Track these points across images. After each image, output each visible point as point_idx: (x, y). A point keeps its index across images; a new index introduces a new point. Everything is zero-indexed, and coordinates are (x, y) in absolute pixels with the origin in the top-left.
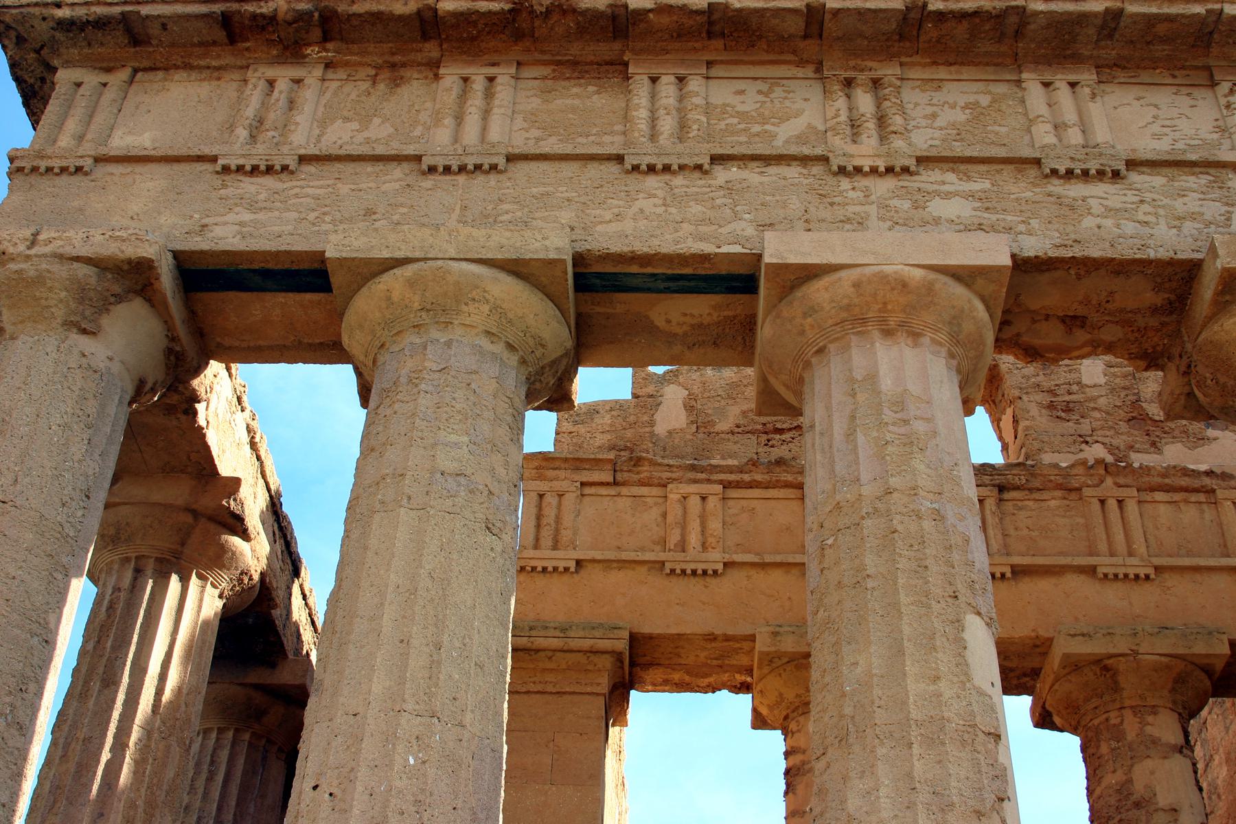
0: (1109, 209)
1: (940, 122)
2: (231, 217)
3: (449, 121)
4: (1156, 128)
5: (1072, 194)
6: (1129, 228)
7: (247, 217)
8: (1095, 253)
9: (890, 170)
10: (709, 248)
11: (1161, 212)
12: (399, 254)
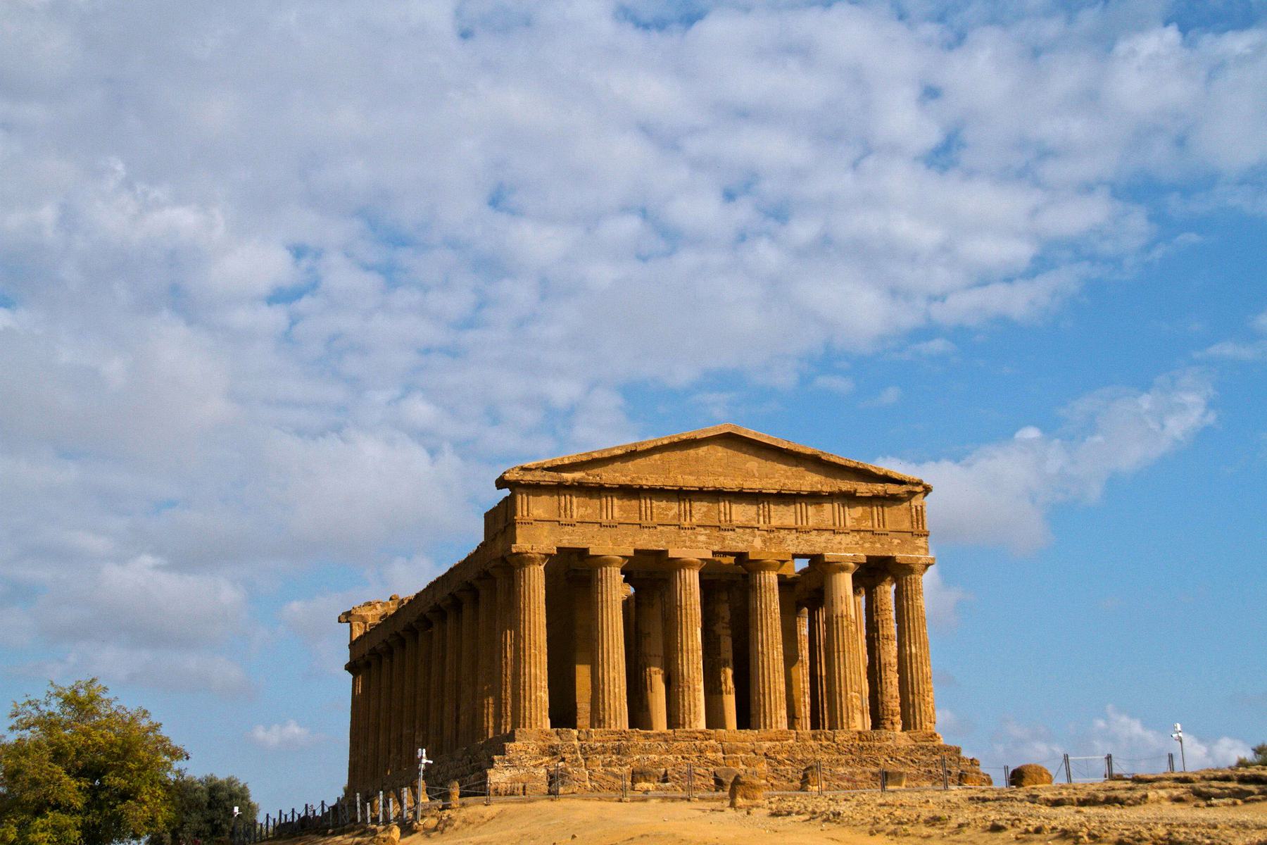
1: (701, 512)
2: (565, 537)
6: (734, 543)
10: (657, 549)
12: (601, 554)
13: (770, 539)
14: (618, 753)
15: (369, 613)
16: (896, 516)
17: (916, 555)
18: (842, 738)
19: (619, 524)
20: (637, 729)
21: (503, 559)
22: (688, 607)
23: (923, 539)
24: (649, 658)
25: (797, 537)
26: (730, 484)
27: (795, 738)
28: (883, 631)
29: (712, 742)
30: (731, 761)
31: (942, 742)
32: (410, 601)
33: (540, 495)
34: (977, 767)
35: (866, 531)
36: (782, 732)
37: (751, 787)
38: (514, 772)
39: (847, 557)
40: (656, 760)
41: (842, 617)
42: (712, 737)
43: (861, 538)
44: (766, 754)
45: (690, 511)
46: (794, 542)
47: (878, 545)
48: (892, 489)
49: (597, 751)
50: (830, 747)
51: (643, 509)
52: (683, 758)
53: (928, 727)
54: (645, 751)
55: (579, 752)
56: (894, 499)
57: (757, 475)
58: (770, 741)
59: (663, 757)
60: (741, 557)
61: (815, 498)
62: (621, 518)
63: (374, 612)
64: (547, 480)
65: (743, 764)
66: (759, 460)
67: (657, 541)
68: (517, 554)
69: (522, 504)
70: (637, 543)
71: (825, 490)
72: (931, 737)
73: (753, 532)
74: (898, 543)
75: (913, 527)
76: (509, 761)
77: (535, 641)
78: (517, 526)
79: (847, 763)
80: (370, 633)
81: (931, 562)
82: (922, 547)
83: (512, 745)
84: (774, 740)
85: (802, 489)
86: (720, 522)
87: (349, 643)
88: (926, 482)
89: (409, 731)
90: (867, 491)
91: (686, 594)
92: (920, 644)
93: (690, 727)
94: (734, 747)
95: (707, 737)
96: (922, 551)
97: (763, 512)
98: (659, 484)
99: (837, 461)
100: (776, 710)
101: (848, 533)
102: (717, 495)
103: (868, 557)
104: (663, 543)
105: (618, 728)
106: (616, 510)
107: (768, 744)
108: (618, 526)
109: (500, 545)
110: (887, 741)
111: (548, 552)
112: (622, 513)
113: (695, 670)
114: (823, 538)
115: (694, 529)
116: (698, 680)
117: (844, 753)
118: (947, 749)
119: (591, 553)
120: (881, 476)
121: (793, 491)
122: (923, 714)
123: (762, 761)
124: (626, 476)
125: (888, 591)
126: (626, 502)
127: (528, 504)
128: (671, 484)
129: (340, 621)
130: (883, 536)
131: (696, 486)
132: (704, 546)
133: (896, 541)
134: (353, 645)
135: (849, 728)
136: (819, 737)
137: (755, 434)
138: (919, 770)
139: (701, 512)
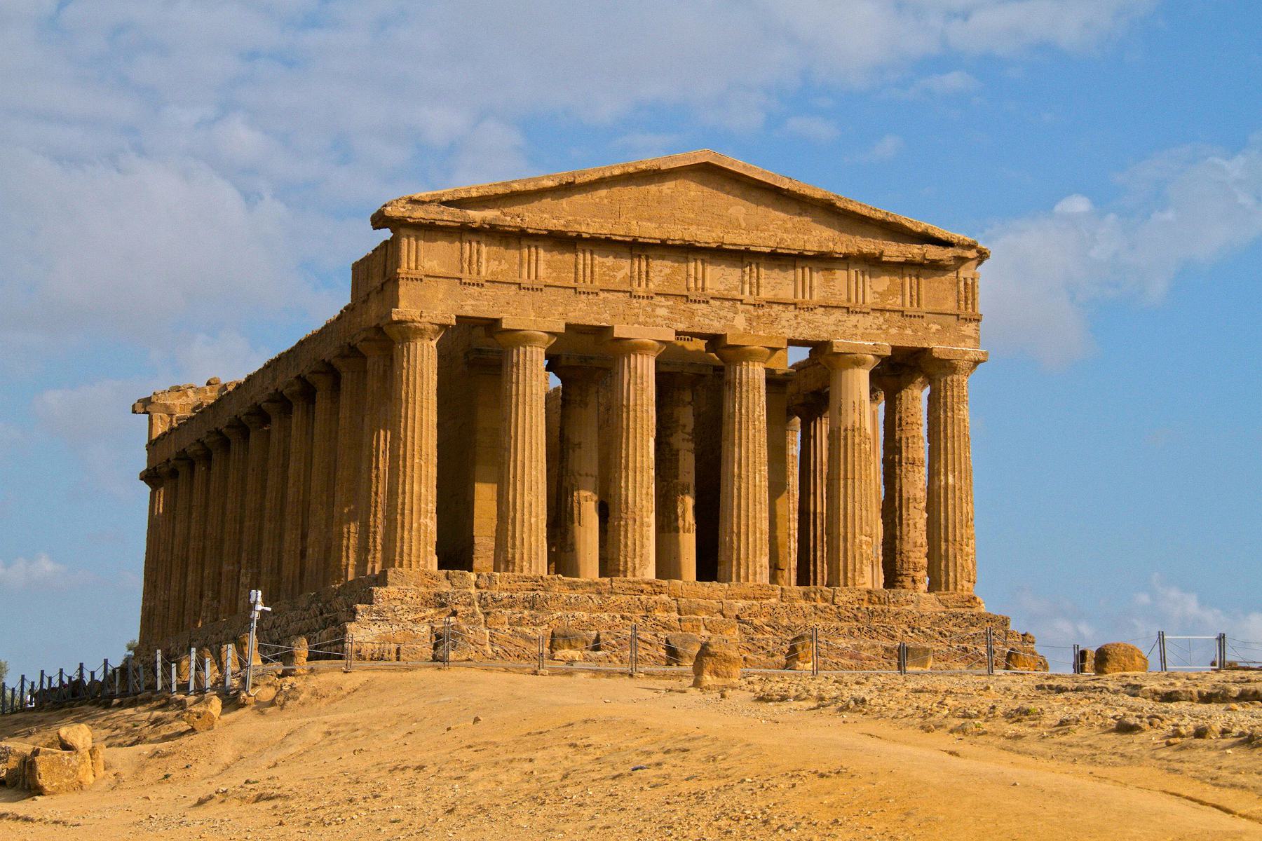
1: (662, 275)
2: (468, 302)
3: (526, 265)
4: (722, 280)
6: (707, 321)
7: (473, 303)
9: (648, 297)
10: (598, 324)
13: (758, 317)
14: (532, 608)
15: (177, 402)
16: (938, 292)
17: (962, 347)
18: (845, 599)
19: (545, 286)
20: (560, 576)
21: (379, 329)
22: (638, 407)
23: (972, 325)
24: (578, 477)
26: (706, 236)
27: (779, 596)
28: (907, 452)
29: (664, 597)
30: (689, 625)
31: (983, 609)
32: (239, 386)
33: (436, 240)
34: (1030, 646)
35: (894, 311)
36: (761, 587)
37: (725, 661)
38: (385, 628)
39: (865, 347)
40: (585, 619)
41: (853, 430)
42: (664, 590)
43: (886, 321)
44: (737, 617)
45: (647, 272)
46: (791, 322)
47: (909, 332)
48: (933, 252)
49: (501, 603)
50: (828, 610)
51: (581, 267)
52: (623, 617)
53: (965, 588)
54: (568, 605)
55: (477, 604)
56: (936, 267)
57: (743, 225)
58: (745, 599)
59: (594, 615)
60: (714, 341)
61: (824, 260)
62: (549, 278)
63: (183, 400)
64: (445, 218)
65: (706, 629)
66: (748, 204)
67: (598, 314)
68: (400, 322)
69: (409, 252)
70: (570, 314)
71: (838, 251)
72: (969, 601)
74: (937, 330)
75: (959, 308)
76: (378, 613)
77: (421, 447)
78: (401, 282)
79: (851, 633)
80: (177, 429)
81: (982, 358)
82: (970, 337)
83: (383, 590)
84: (750, 598)
85: (807, 248)
86: (688, 290)
87: (146, 442)
88: (981, 245)
89: (231, 568)
90: (897, 254)
91: (636, 390)
92: (960, 472)
93: (634, 576)
94: (694, 606)
95: (657, 590)
96: (970, 342)
97: (750, 277)
98: (606, 232)
99: (858, 209)
100: (755, 557)
101: (868, 313)
102: (687, 251)
103: (894, 349)
104: (607, 316)
105: (533, 573)
106: (542, 266)
107: (741, 603)
108: (544, 289)
109: (374, 309)
110: (907, 605)
111: (444, 321)
112: (550, 270)
113: (644, 496)
114: (832, 319)
115: (652, 298)
116: (648, 511)
117: (847, 619)
118: (990, 619)
119: (504, 326)
120: (919, 233)
121: (795, 250)
122: (959, 570)
123: (733, 626)
124: (558, 218)
125: (917, 398)
126: (557, 256)
127: (417, 252)
128: (622, 233)
129: (134, 412)
130: (917, 319)
131: (657, 236)
132: (665, 322)
133: (934, 327)
134: (152, 445)
135: (855, 584)
136: (813, 595)
137: (744, 166)
138: (951, 646)
139: (662, 275)
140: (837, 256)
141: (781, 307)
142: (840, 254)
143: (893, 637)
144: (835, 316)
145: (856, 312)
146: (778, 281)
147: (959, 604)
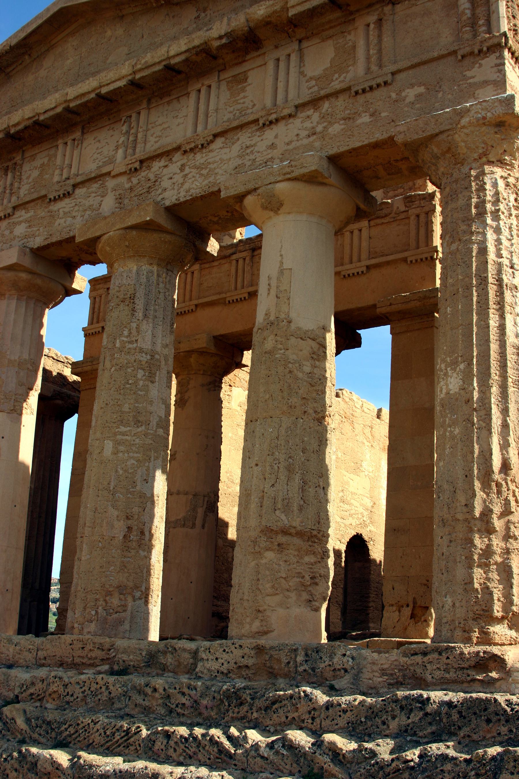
0: (65, 213)
5: (56, 209)
8: (54, 240)
9: (5, 216)
11: (81, 209)
13: (131, 189)
25: (183, 165)
35: (336, 94)
47: (365, 119)
73: (103, 186)
74: (419, 96)
85: (172, 53)
101: (290, 116)
114: (236, 148)
140: (216, 44)
141: (163, 163)
142: (221, 37)
143: (231, 756)
144: (239, 142)
145: (271, 122)
146: (165, 126)
147: (452, 675)
